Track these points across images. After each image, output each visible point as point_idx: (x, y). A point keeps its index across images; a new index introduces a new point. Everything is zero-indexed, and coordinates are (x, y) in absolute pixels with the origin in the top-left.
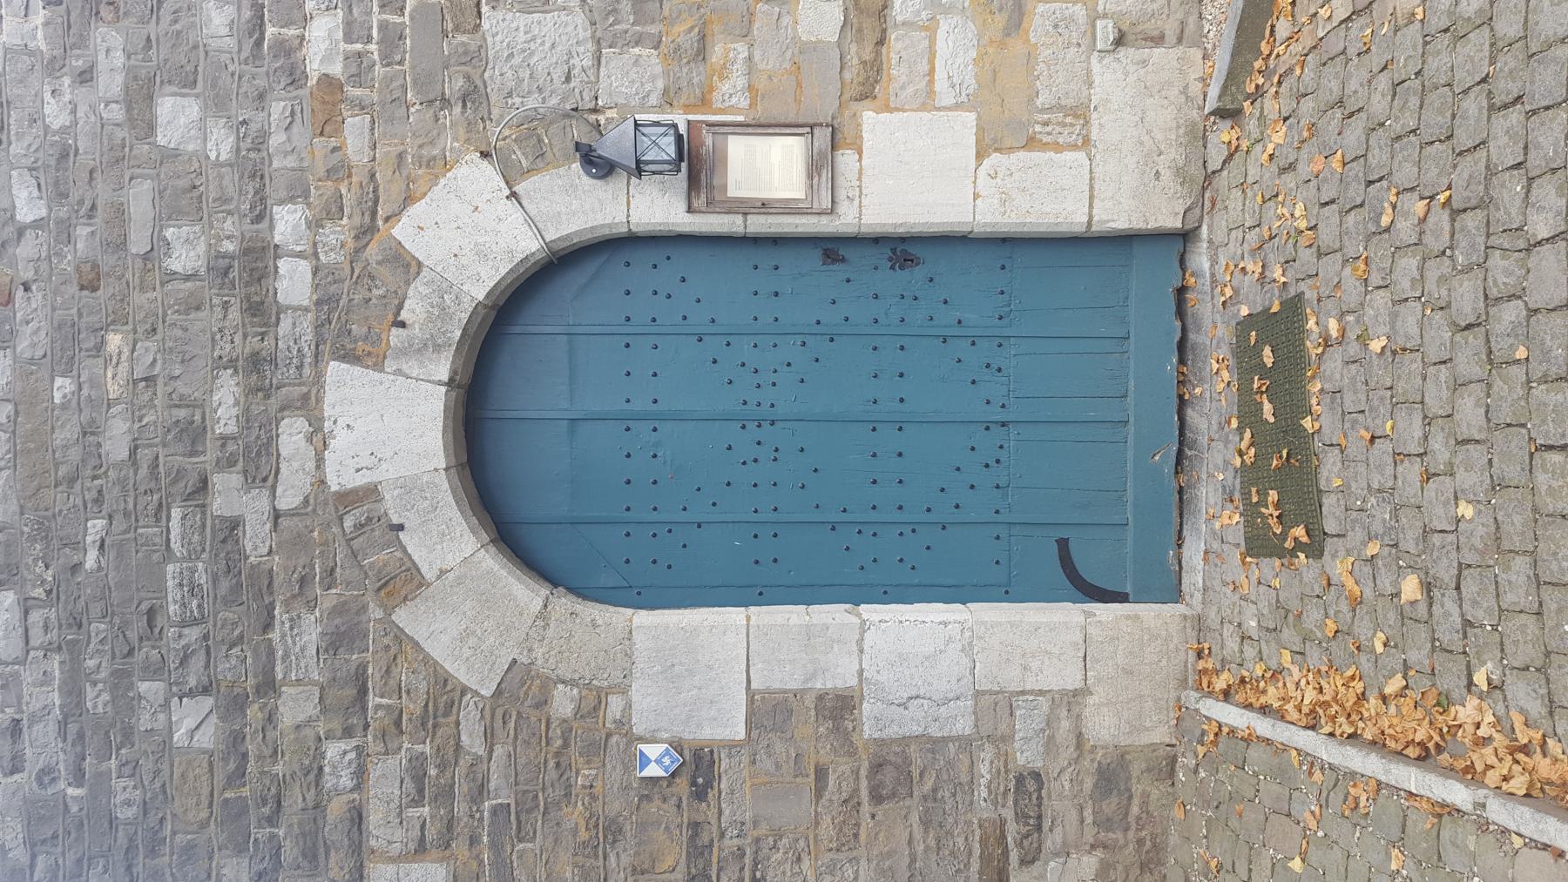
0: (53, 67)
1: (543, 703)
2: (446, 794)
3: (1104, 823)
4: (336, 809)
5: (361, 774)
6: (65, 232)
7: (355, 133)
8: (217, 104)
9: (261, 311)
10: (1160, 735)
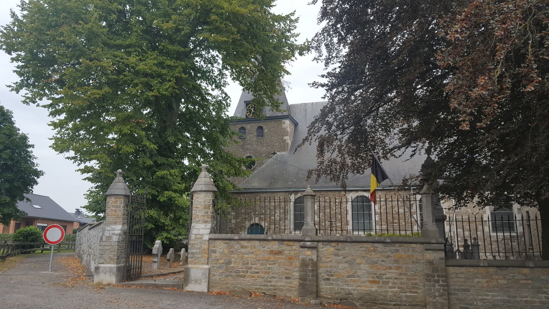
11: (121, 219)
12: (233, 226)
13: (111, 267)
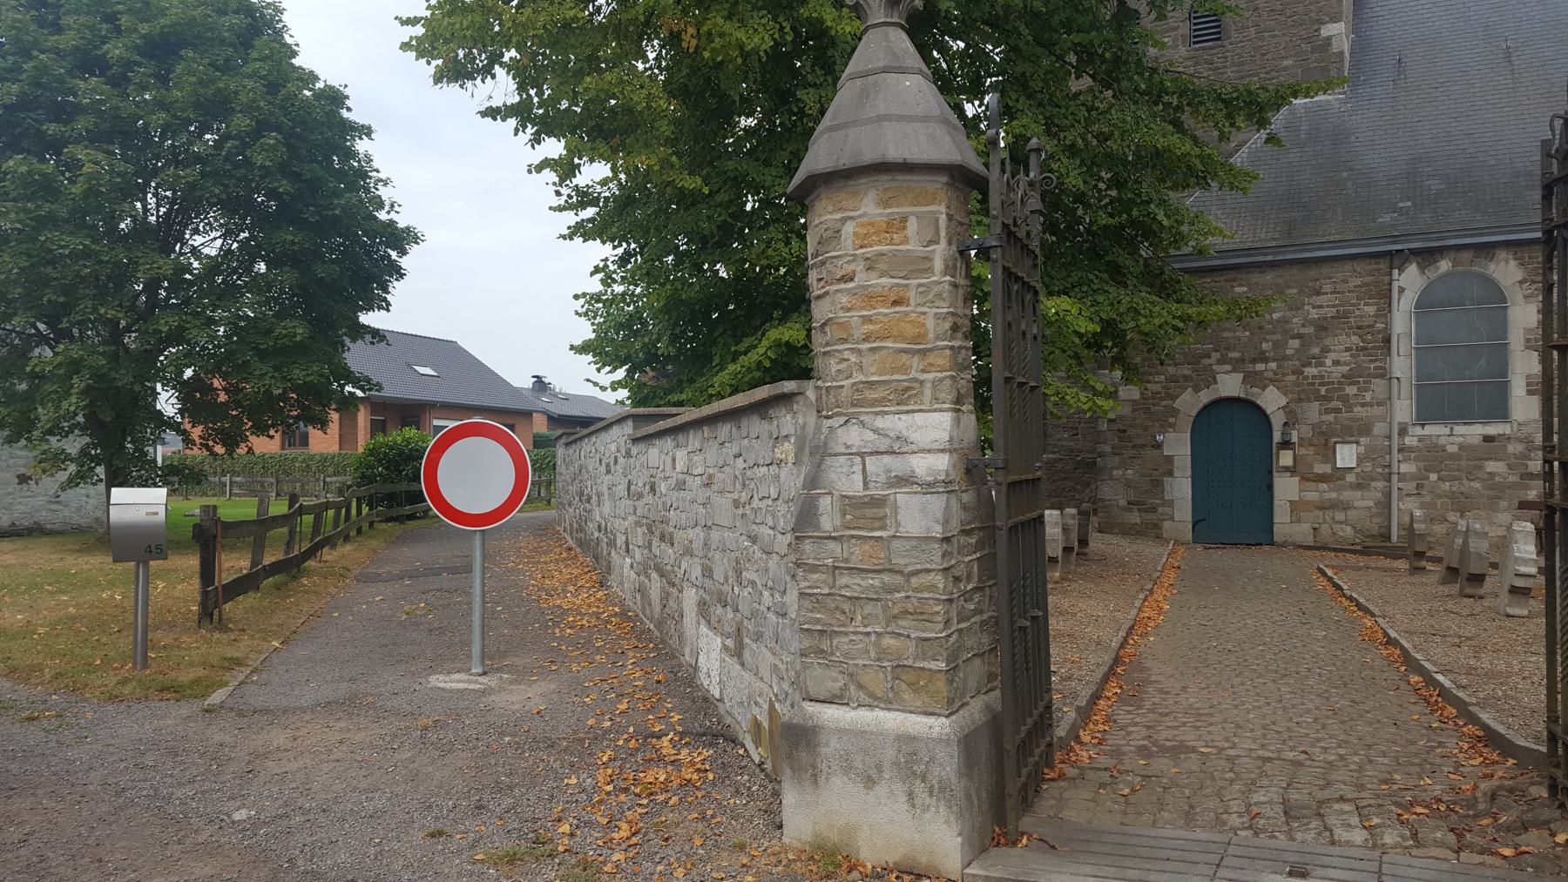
0: (1305, 319)
1: (1172, 416)
2: (1153, 398)
3: (1146, 524)
4: (1151, 378)
5: (1158, 382)
6: (1270, 323)
7: (1294, 377)
8: (1297, 351)
9: (1254, 361)
10: (1165, 536)
11: (943, 359)
12: (1125, 410)
13: (912, 739)
